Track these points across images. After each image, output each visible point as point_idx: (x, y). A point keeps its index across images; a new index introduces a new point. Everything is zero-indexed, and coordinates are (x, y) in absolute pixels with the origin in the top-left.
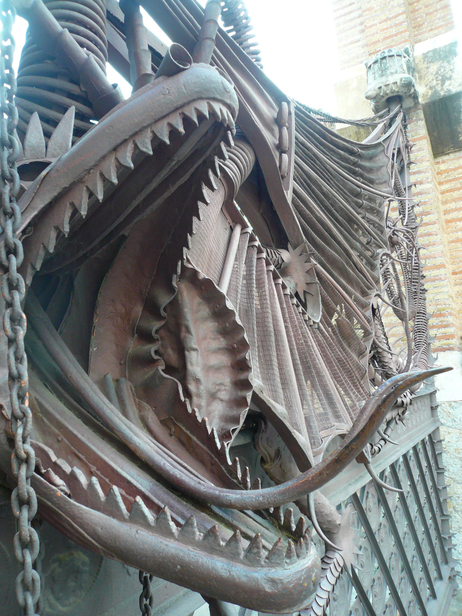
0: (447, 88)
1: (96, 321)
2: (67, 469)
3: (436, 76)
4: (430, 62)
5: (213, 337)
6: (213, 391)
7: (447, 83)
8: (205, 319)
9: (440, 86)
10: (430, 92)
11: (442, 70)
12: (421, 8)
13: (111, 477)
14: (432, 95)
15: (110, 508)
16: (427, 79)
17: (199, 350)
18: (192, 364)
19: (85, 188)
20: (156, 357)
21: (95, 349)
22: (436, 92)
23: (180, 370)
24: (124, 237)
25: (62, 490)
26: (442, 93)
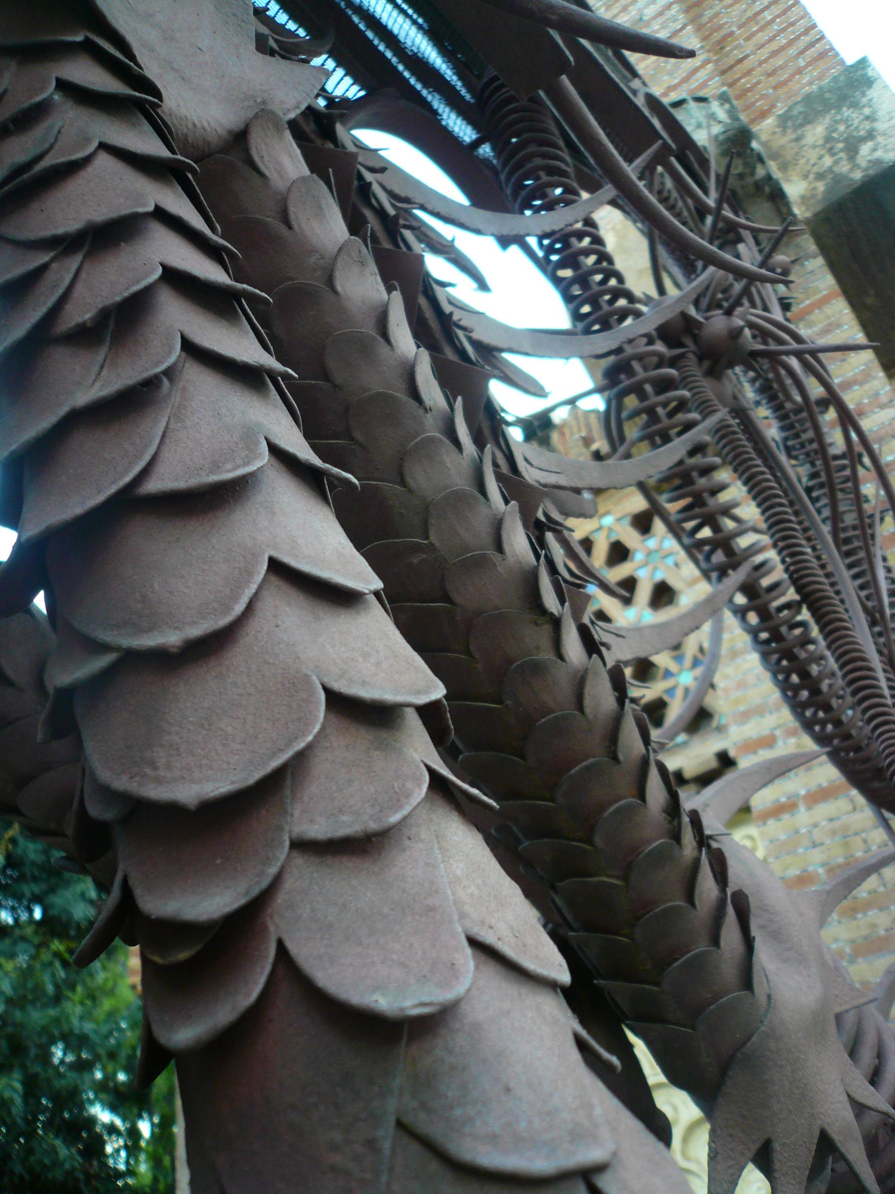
0: (869, 158)
3: (828, 146)
4: (801, 125)
7: (865, 149)
9: (844, 162)
10: (821, 186)
11: (841, 128)
12: (758, 83)
14: (829, 190)
16: (802, 161)
22: (838, 179)
26: (858, 175)
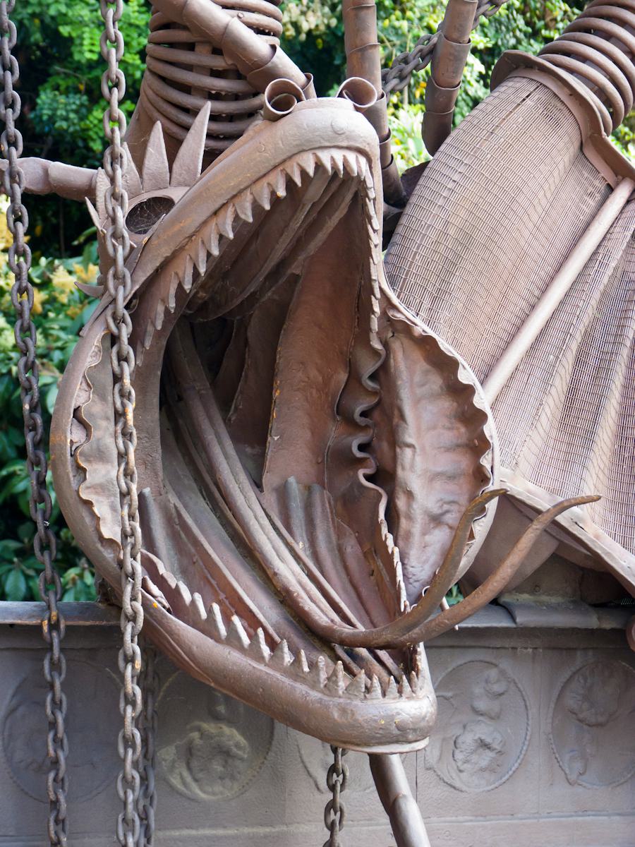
1: (277, 394)
2: (173, 582)
5: (447, 424)
6: (436, 510)
8: (434, 397)
13: (235, 605)
15: (208, 628)
17: (417, 446)
18: (403, 468)
19: (188, 257)
20: (359, 455)
21: (276, 438)
23: (386, 477)
24: (295, 278)
25: (160, 602)
